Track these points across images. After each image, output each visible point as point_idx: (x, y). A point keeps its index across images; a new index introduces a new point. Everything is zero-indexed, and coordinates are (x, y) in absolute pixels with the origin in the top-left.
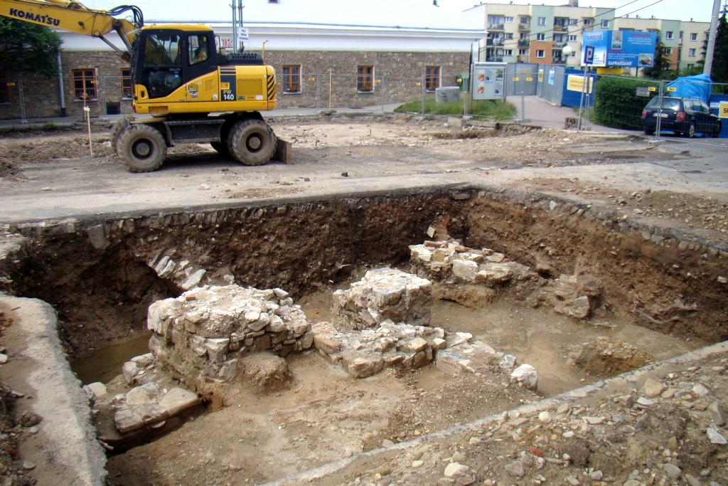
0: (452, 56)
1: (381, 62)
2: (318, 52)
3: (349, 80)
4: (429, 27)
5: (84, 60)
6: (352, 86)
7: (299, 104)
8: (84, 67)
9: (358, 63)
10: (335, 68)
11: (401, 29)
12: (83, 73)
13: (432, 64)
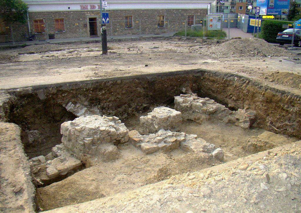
0: (199, 11)
1: (168, 14)
2: (140, 10)
3: (154, 22)
6: (155, 24)
7: (132, 33)
8: (39, 19)
10: (148, 17)
12: (38, 21)
13: (190, 14)
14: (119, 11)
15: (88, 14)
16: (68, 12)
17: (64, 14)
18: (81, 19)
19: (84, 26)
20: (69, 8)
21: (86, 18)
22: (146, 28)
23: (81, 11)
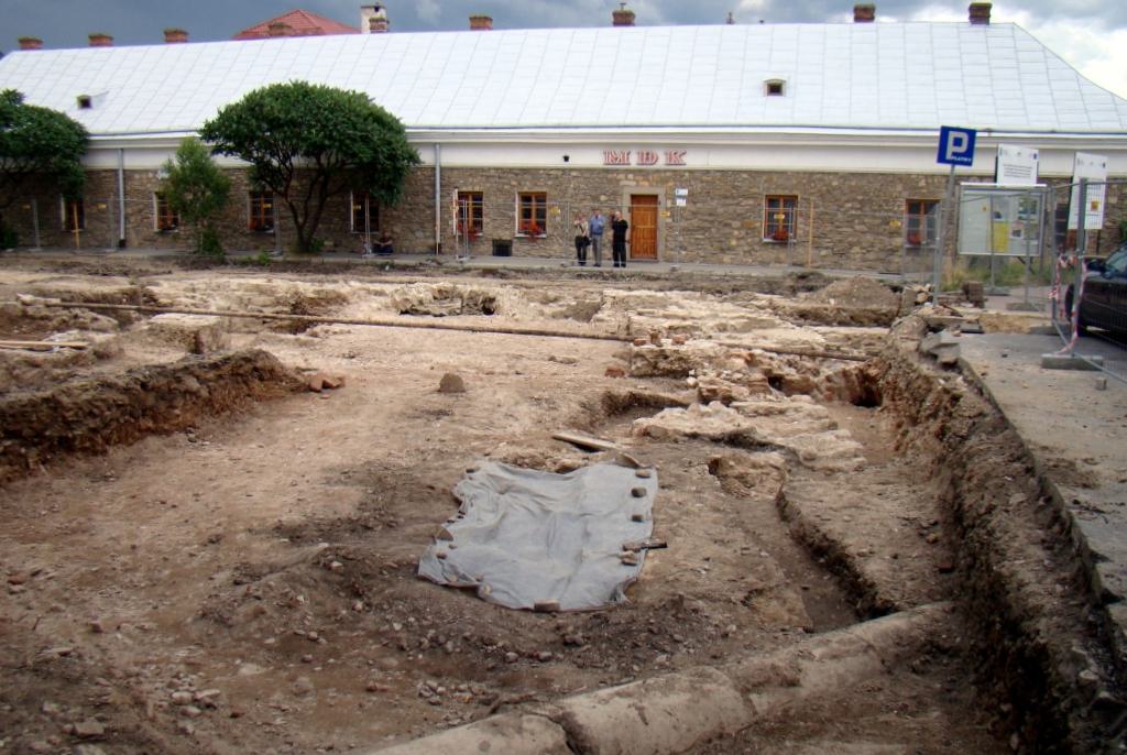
2: (829, 173)
4: (1057, 128)
5: (470, 180)
9: (905, 195)
10: (860, 202)
11: (993, 135)
12: (533, 199)
14: (745, 176)
15: (627, 183)
16: (563, 170)
17: (550, 179)
18: (603, 198)
20: (566, 159)
21: (621, 195)
22: (851, 245)
23: (607, 171)
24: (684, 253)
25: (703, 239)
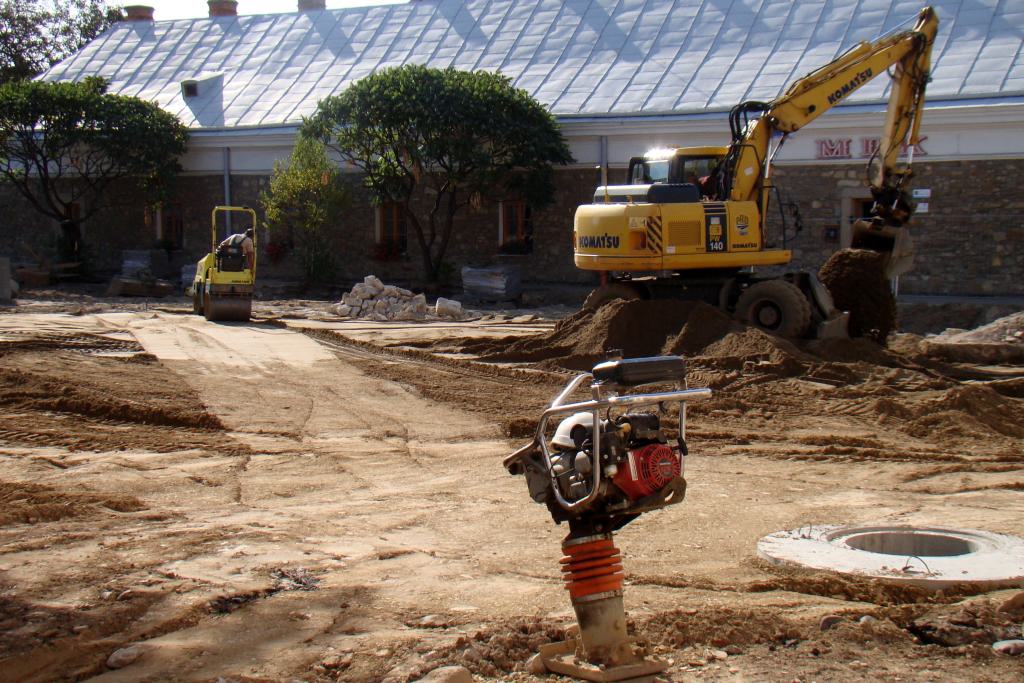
15: (848, 183)
18: (815, 205)
19: (828, 235)
21: (839, 201)
23: (822, 168)
24: (926, 278)
25: (953, 259)
